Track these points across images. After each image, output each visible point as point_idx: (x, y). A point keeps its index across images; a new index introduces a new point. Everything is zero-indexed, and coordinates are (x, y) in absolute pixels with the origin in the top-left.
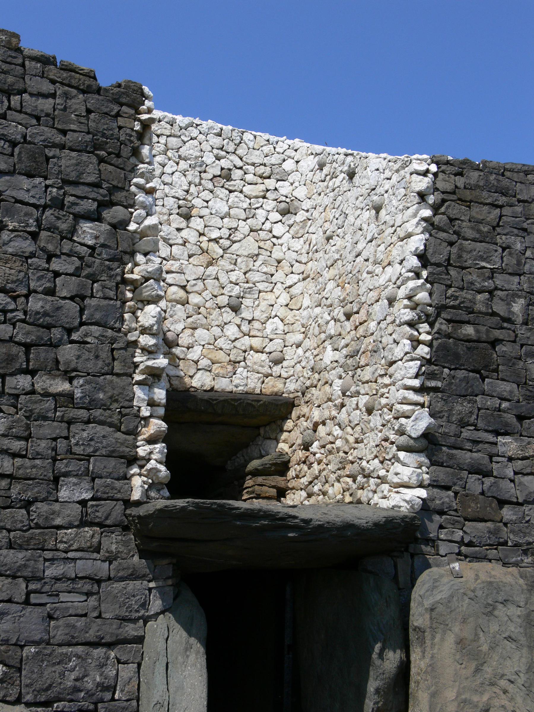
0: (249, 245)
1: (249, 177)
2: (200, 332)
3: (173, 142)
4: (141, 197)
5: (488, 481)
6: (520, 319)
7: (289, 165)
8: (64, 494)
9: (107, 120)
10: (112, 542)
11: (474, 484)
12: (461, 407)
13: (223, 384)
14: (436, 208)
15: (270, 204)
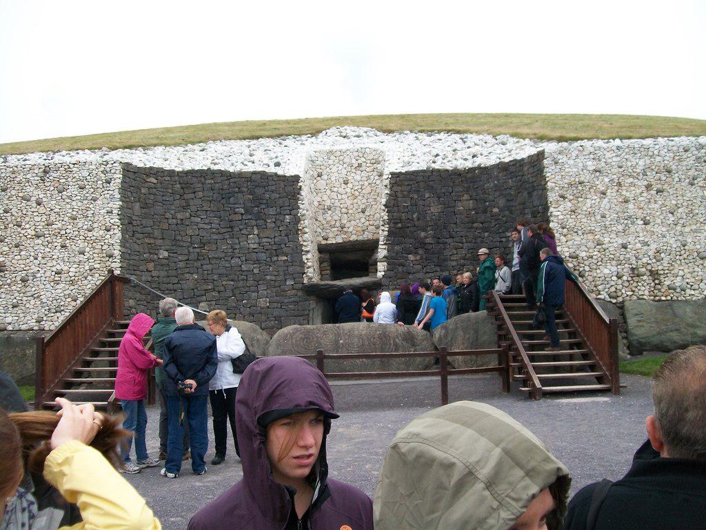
0: (369, 189)
1: (368, 165)
2: (353, 222)
3: (341, 158)
4: (301, 206)
5: (405, 268)
6: (415, 220)
7: (381, 159)
8: (288, 283)
9: (290, 187)
10: (300, 293)
11: (400, 269)
12: (397, 248)
13: (360, 238)
14: (391, 188)
15: (375, 173)
